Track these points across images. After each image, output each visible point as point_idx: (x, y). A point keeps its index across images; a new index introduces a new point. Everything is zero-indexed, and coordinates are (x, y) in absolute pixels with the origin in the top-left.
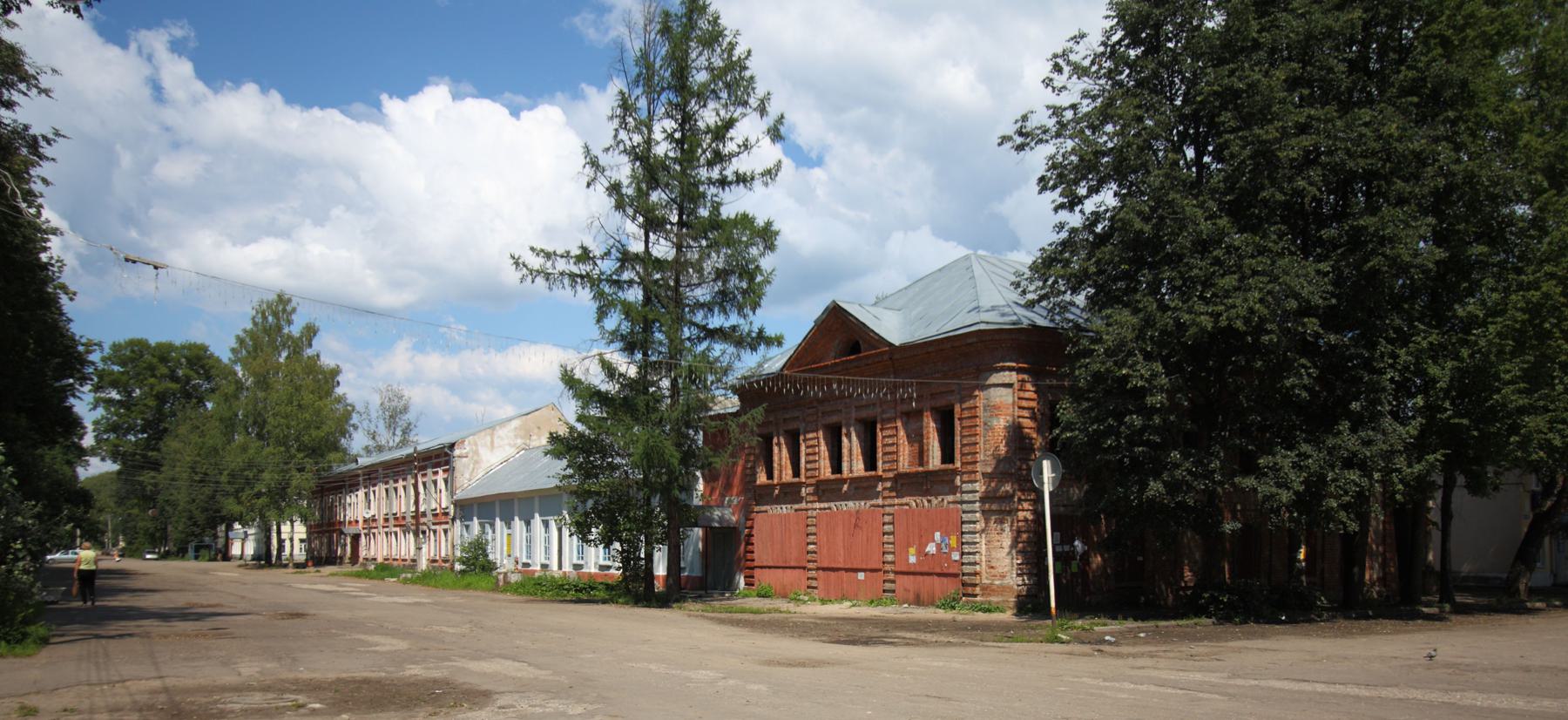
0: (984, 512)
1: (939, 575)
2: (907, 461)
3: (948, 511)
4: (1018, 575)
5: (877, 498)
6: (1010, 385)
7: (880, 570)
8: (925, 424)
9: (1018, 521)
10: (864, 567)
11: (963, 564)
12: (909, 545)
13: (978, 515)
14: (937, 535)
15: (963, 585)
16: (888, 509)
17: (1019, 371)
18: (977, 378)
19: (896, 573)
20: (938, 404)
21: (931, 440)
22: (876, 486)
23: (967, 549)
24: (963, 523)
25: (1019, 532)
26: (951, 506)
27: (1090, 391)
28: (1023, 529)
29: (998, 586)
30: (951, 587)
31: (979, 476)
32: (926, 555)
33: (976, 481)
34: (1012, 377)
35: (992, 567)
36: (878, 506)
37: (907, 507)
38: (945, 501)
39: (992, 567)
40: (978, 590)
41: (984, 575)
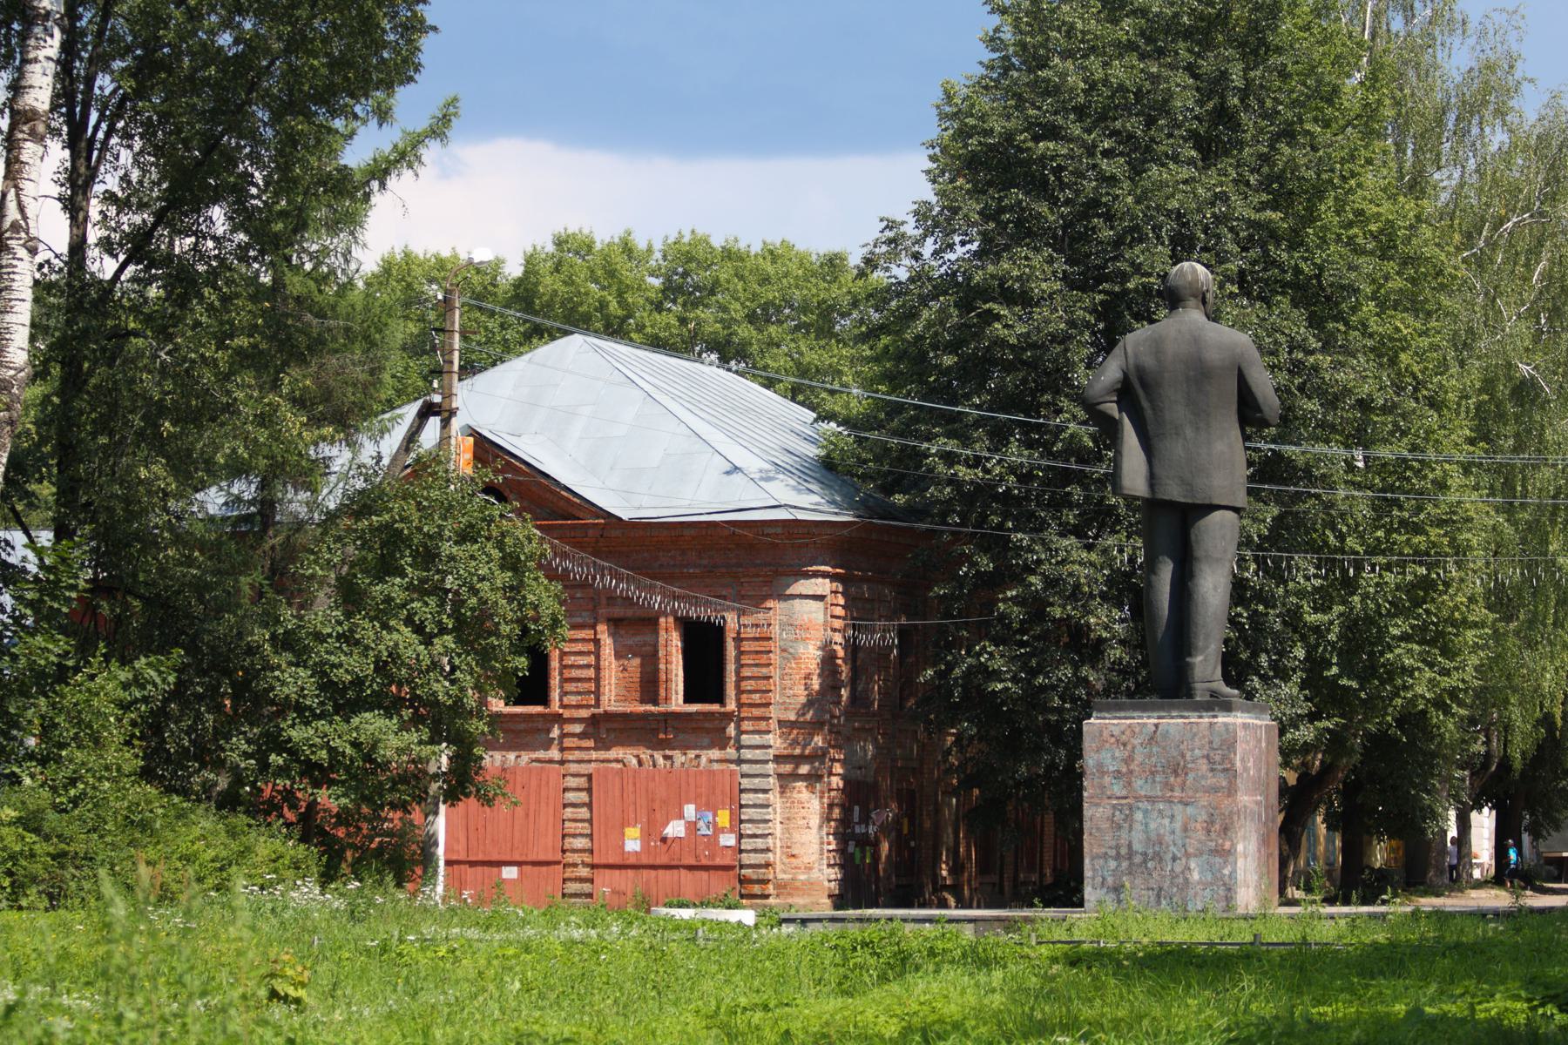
0: (780, 776)
1: (690, 868)
2: (613, 693)
3: (712, 773)
4: (829, 865)
5: (547, 748)
6: (821, 598)
7: (558, 863)
8: (662, 641)
9: (830, 790)
10: (517, 858)
11: (741, 851)
12: (625, 824)
13: (771, 780)
14: (690, 810)
15: (741, 882)
16: (574, 768)
17: (834, 578)
18: (768, 583)
19: (593, 866)
20: (693, 614)
21: (674, 666)
22: (549, 731)
23: (748, 829)
24: (742, 791)
25: (831, 806)
26: (716, 766)
27: (1023, 631)
28: (836, 801)
29: (803, 883)
30: (721, 884)
31: (773, 725)
32: (664, 840)
33: (769, 732)
34: (823, 586)
35: (793, 856)
36: (551, 761)
37: (620, 766)
38: (704, 760)
39: (793, 856)
40: (770, 889)
41: (779, 867)
